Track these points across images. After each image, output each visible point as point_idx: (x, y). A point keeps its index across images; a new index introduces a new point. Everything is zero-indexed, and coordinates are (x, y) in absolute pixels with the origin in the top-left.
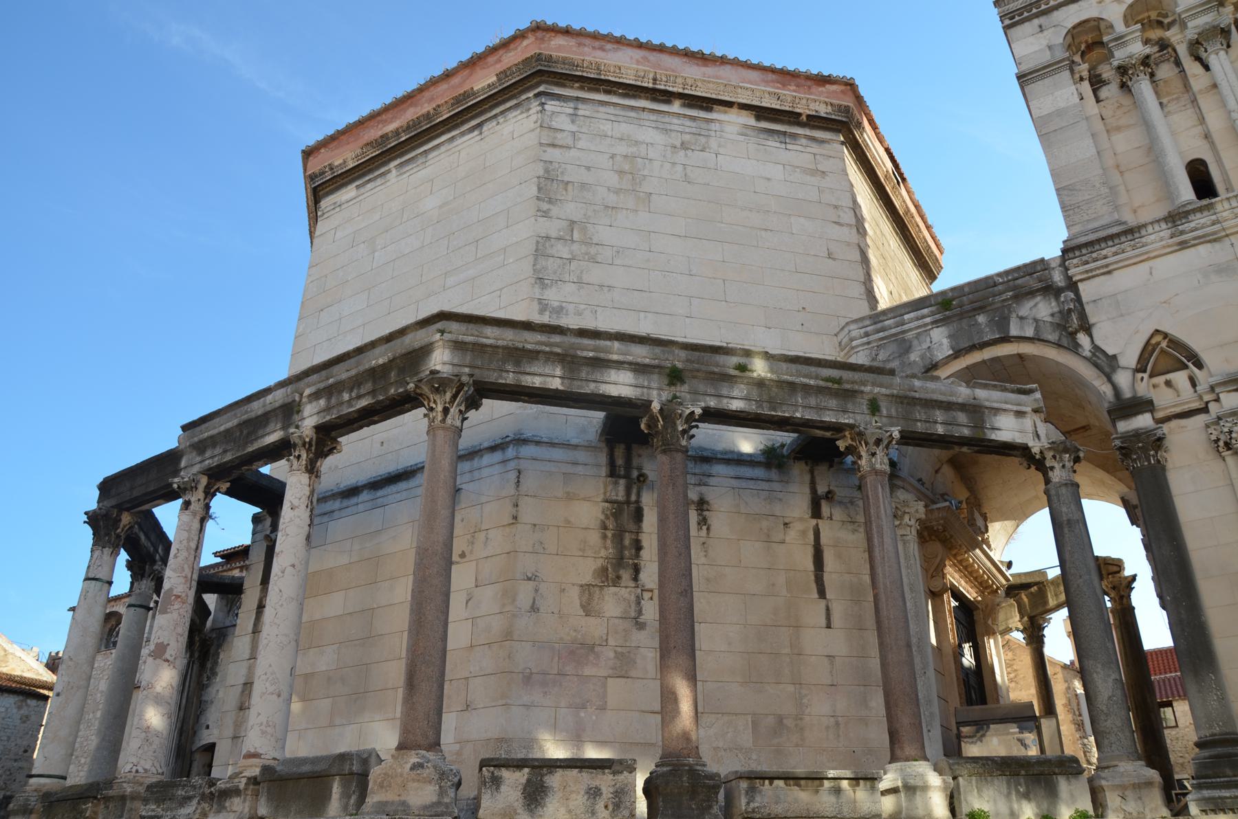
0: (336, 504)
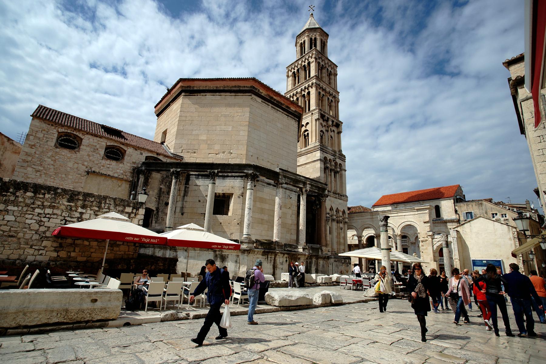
0: (266, 185)
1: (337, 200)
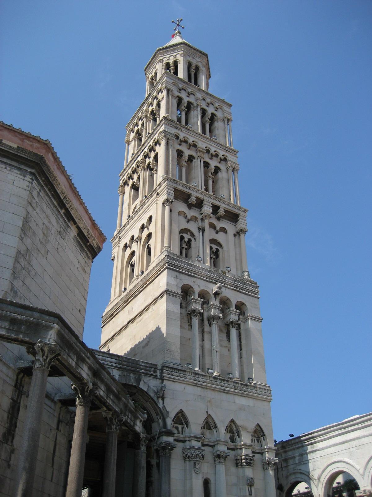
1: (230, 397)
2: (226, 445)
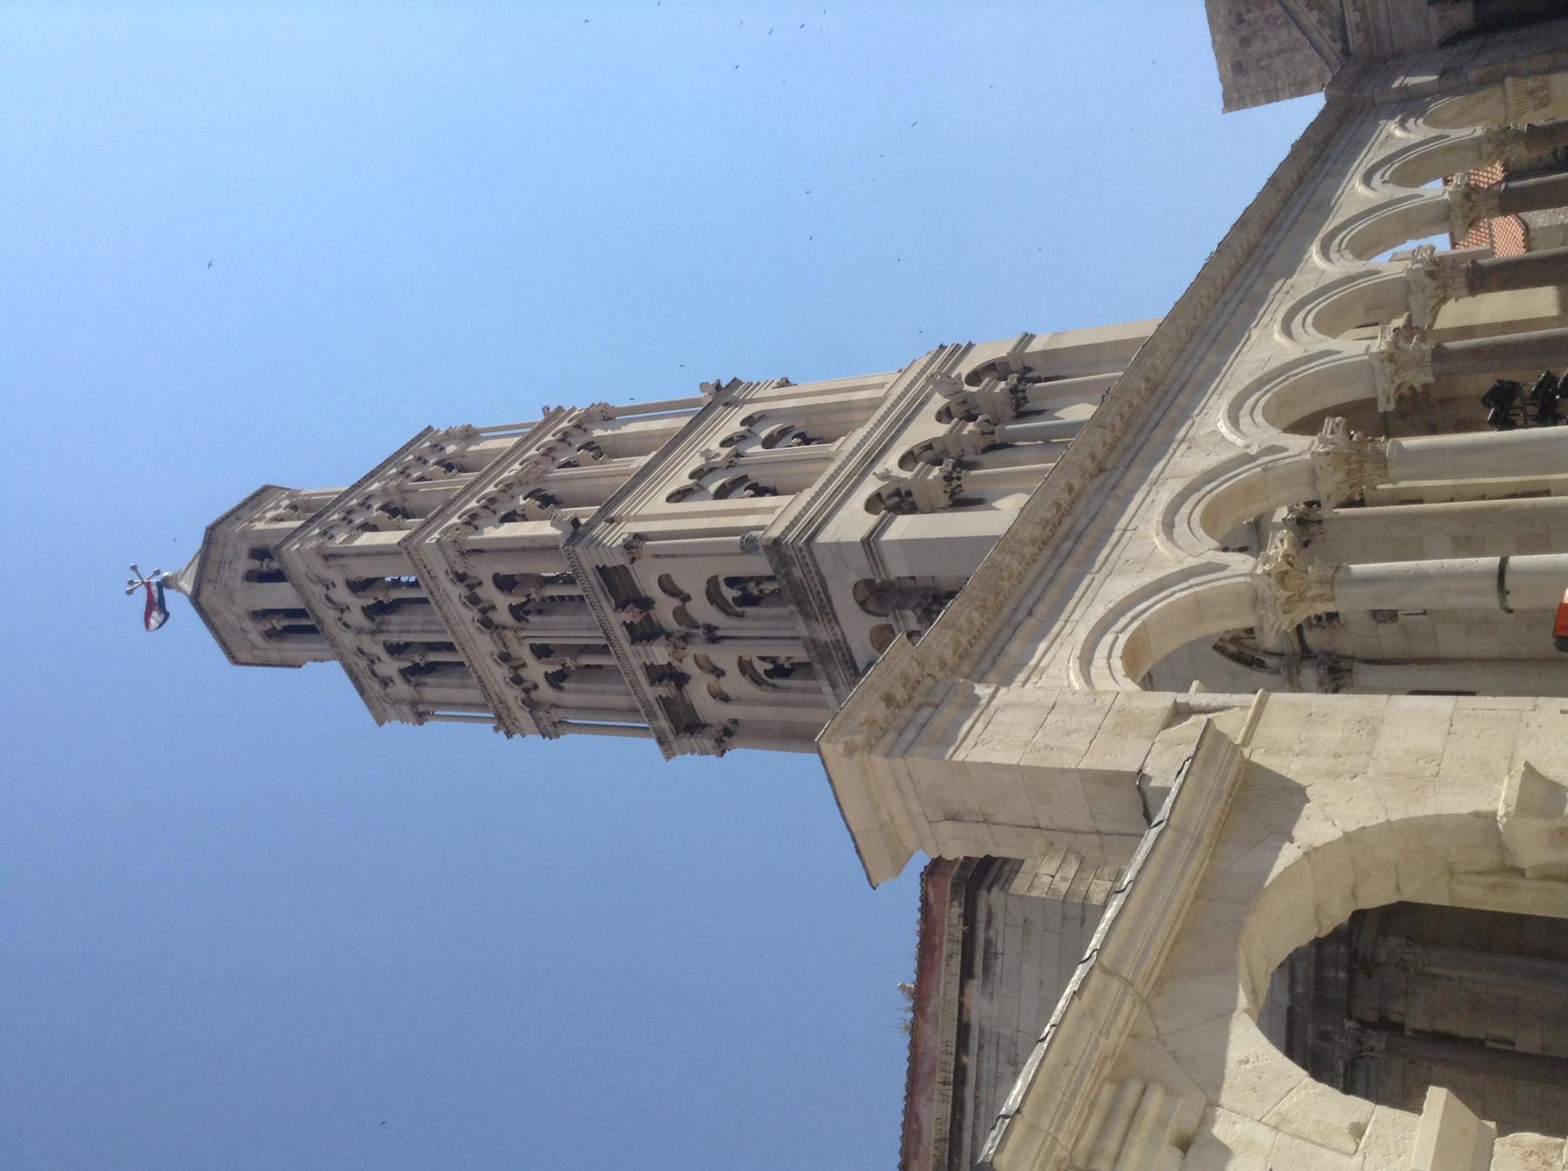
2: (1299, 672)
